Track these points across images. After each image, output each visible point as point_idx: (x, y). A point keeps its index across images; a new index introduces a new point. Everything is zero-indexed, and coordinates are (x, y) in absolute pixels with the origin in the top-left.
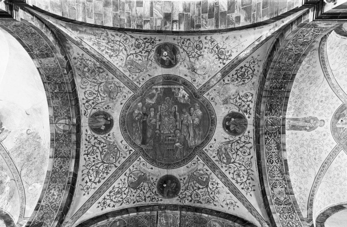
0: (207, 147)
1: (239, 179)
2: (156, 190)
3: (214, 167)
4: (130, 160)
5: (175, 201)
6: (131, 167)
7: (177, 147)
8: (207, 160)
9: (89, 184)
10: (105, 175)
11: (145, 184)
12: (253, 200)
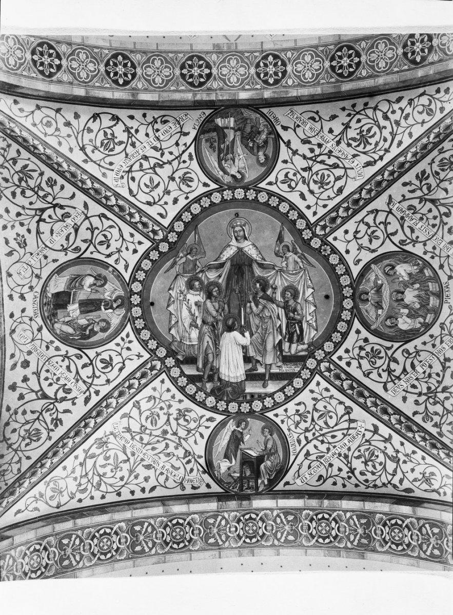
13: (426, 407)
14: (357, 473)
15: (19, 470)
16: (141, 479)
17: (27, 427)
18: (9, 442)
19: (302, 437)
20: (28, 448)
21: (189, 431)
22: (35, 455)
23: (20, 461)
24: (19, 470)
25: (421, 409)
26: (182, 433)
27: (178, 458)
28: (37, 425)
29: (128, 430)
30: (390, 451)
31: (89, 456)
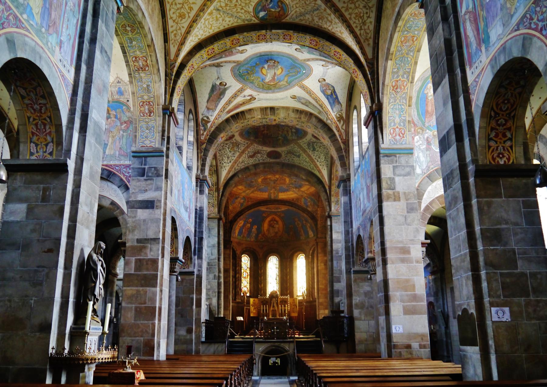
0: (300, 141)
1: (319, 160)
2: (265, 156)
3: (305, 151)
4: (248, 147)
5: (278, 160)
6: (249, 150)
7: (279, 139)
8: (300, 147)
9: (225, 164)
10: (233, 158)
11: (259, 155)
12: (325, 173)
13: (348, 5)
14: (315, 21)
15: (181, 34)
16: (227, 21)
17: (179, 11)
18: (174, 19)
19: (294, 6)
20: (182, 22)
21: (246, 4)
22: (186, 25)
23: (180, 29)
24: (181, 34)
25: (345, 5)
26: (243, 5)
27: (242, 13)
28: (182, 10)
29: (221, 7)
30: (329, 19)
31: (205, 20)
